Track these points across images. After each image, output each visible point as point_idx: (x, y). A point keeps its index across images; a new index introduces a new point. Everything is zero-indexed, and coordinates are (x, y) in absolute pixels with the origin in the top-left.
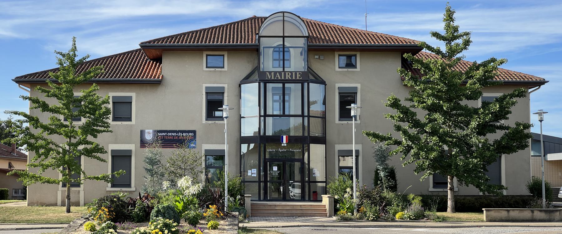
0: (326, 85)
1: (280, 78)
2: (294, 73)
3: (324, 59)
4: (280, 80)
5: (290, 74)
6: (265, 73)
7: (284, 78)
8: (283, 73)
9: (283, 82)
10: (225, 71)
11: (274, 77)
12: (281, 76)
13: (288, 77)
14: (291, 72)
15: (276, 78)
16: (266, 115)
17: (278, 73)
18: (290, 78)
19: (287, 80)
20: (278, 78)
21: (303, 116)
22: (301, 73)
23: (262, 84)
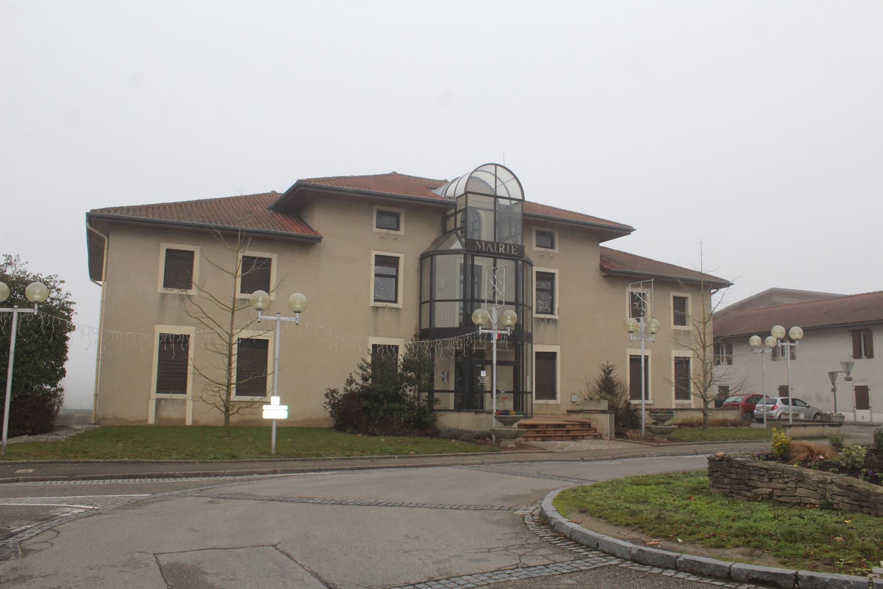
1: (491, 251)
2: (508, 246)
4: (489, 253)
5: (504, 247)
8: (495, 245)
9: (495, 256)
11: (486, 249)
12: (493, 249)
13: (502, 250)
14: (506, 245)
17: (489, 245)
18: (504, 252)
19: (499, 254)
20: (489, 249)
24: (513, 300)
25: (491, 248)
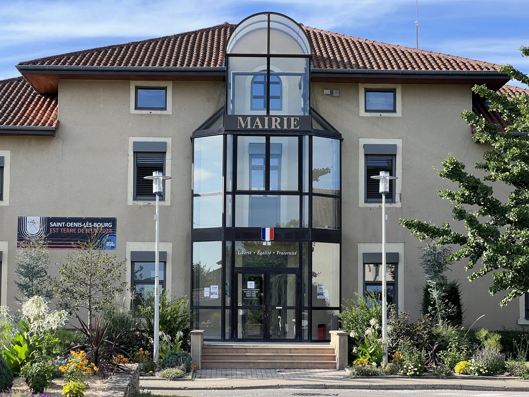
0: (341, 140)
1: (261, 127)
2: (285, 119)
3: (339, 97)
6: (235, 118)
8: (266, 119)
9: (266, 133)
10: (169, 115)
11: (252, 126)
12: (263, 125)
13: (275, 125)
14: (281, 117)
15: (254, 128)
16: (235, 192)
18: (279, 127)
19: (273, 131)
21: (300, 193)
22: (298, 118)
23: (230, 138)
24: (296, 189)
25: (259, 124)
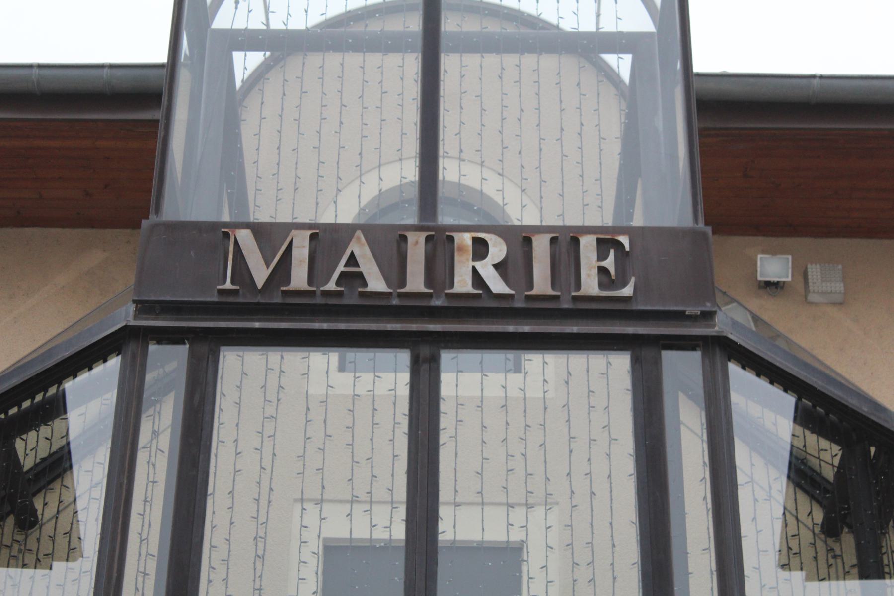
1: (376, 283)
2: (541, 247)
5: (498, 250)
7: (429, 280)
18: (497, 285)
20: (353, 278)
22: (625, 240)
